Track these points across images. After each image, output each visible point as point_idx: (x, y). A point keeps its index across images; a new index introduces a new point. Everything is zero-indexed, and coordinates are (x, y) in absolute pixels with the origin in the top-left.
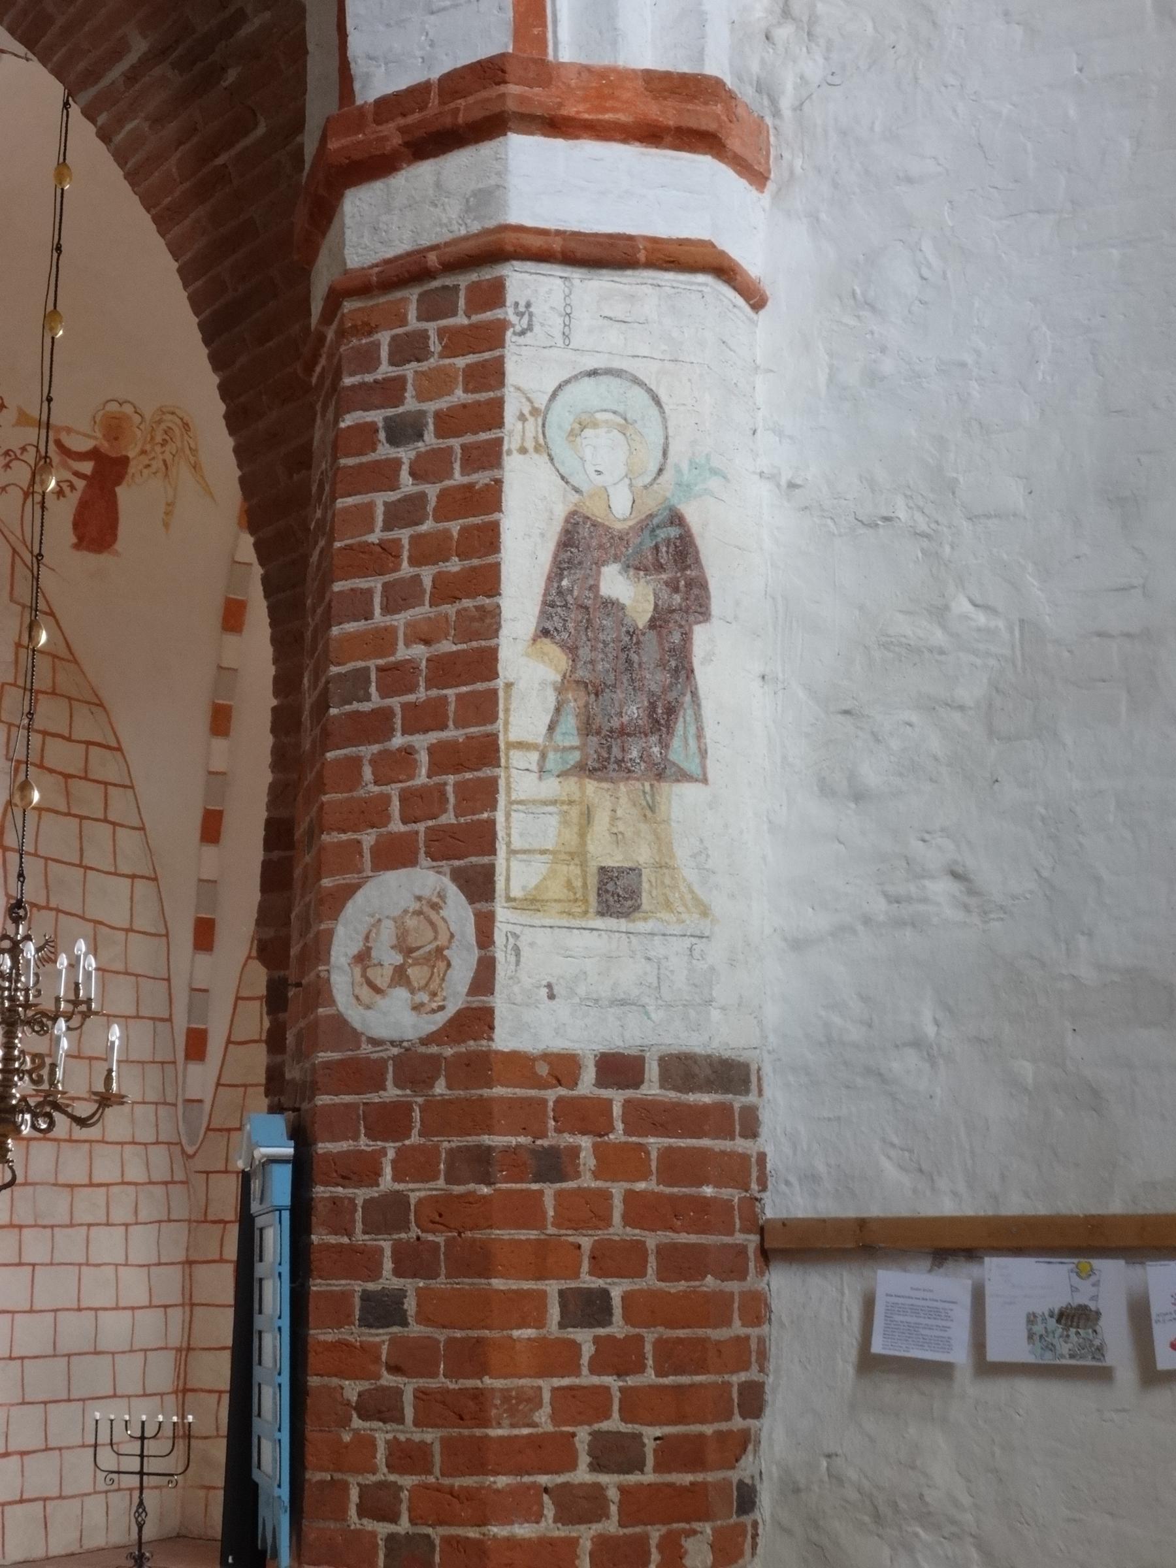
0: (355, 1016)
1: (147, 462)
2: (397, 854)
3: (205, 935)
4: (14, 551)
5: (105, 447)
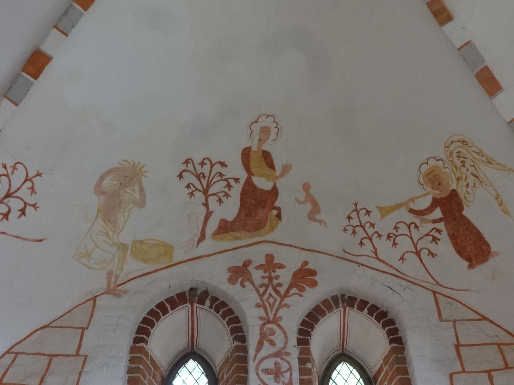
1: (465, 184)
4: (434, 293)
5: (437, 193)
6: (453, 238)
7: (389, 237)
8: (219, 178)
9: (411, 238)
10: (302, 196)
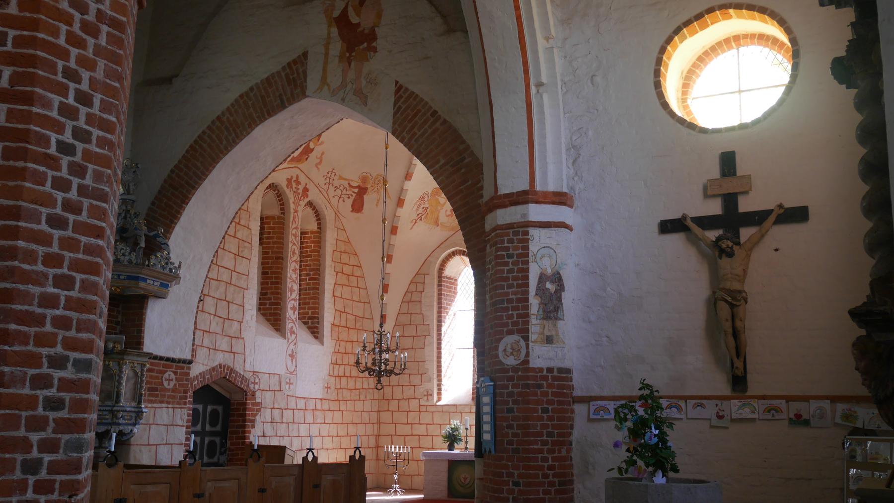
0: (503, 361)
2: (510, 332)
5: (361, 185)
10: (319, 156)
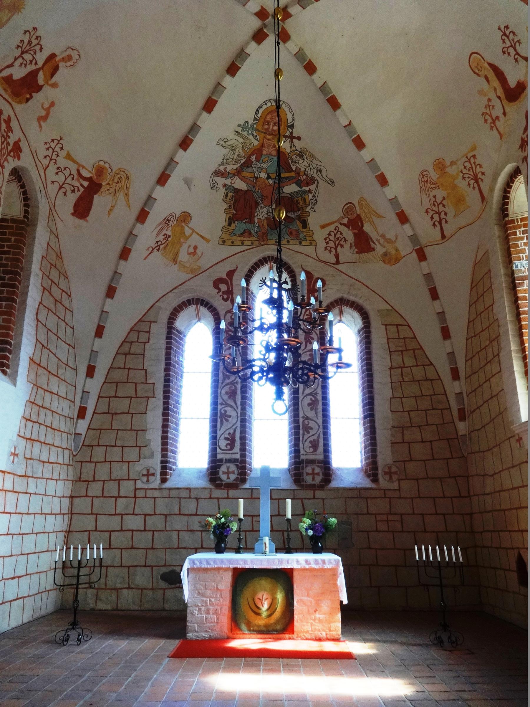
1: (108, 188)
3: (91, 372)
6: (80, 199)
7: (58, 168)
8: (33, 53)
9: (66, 179)
10: (46, 105)
